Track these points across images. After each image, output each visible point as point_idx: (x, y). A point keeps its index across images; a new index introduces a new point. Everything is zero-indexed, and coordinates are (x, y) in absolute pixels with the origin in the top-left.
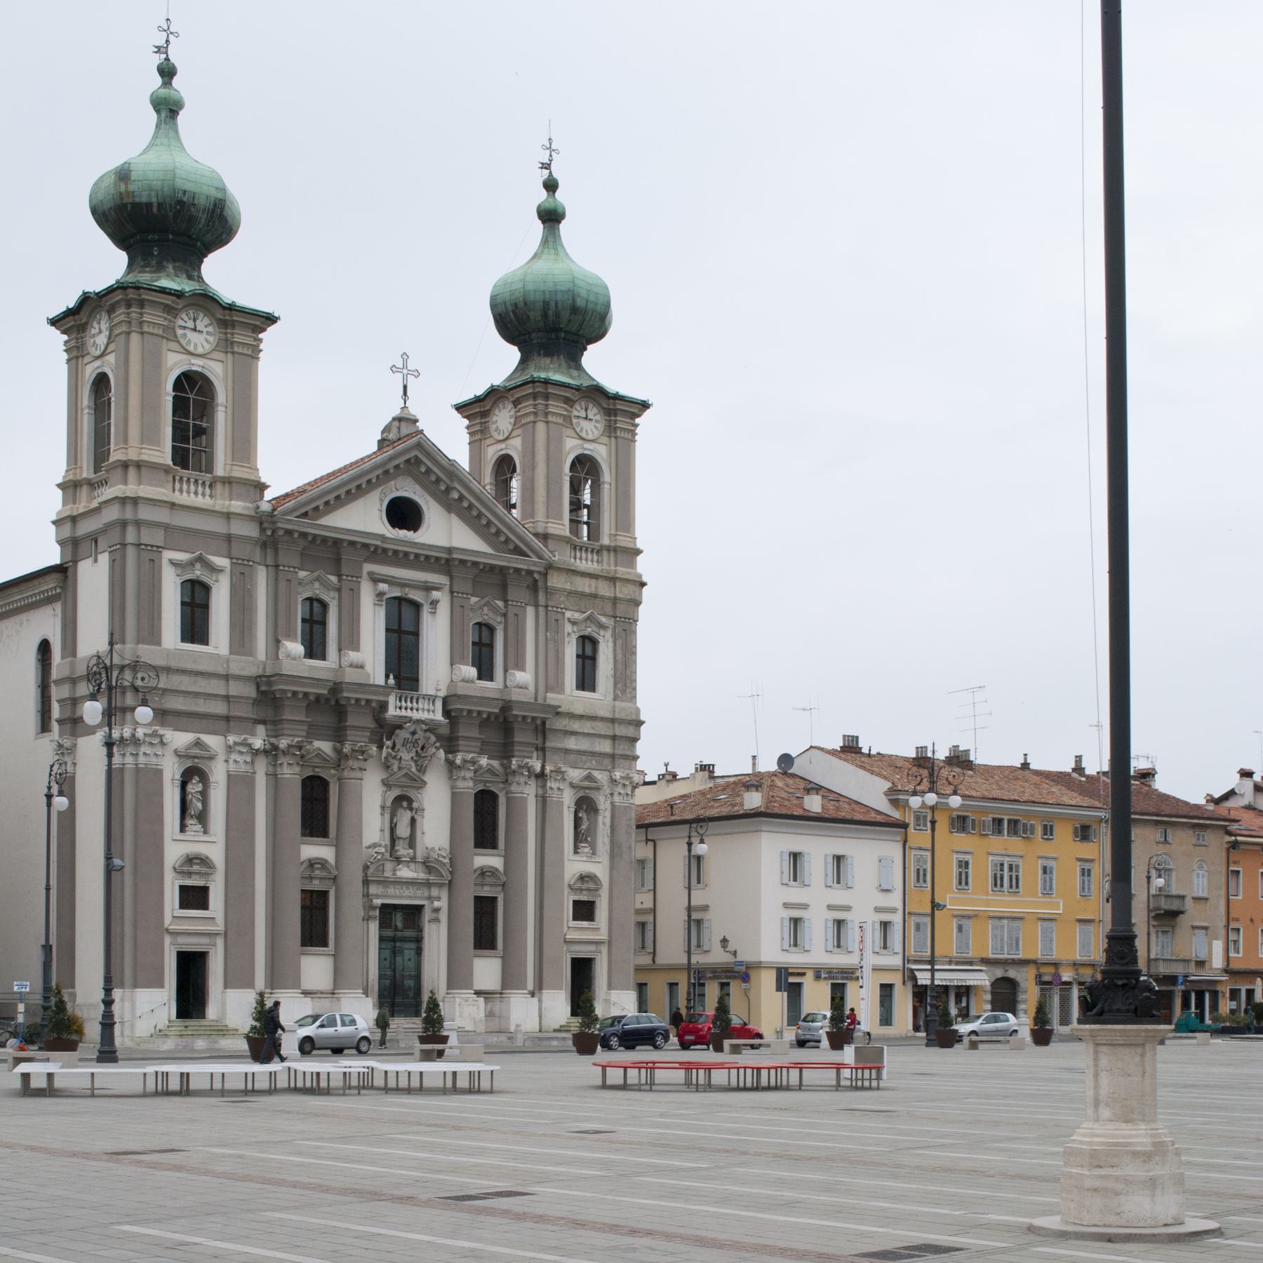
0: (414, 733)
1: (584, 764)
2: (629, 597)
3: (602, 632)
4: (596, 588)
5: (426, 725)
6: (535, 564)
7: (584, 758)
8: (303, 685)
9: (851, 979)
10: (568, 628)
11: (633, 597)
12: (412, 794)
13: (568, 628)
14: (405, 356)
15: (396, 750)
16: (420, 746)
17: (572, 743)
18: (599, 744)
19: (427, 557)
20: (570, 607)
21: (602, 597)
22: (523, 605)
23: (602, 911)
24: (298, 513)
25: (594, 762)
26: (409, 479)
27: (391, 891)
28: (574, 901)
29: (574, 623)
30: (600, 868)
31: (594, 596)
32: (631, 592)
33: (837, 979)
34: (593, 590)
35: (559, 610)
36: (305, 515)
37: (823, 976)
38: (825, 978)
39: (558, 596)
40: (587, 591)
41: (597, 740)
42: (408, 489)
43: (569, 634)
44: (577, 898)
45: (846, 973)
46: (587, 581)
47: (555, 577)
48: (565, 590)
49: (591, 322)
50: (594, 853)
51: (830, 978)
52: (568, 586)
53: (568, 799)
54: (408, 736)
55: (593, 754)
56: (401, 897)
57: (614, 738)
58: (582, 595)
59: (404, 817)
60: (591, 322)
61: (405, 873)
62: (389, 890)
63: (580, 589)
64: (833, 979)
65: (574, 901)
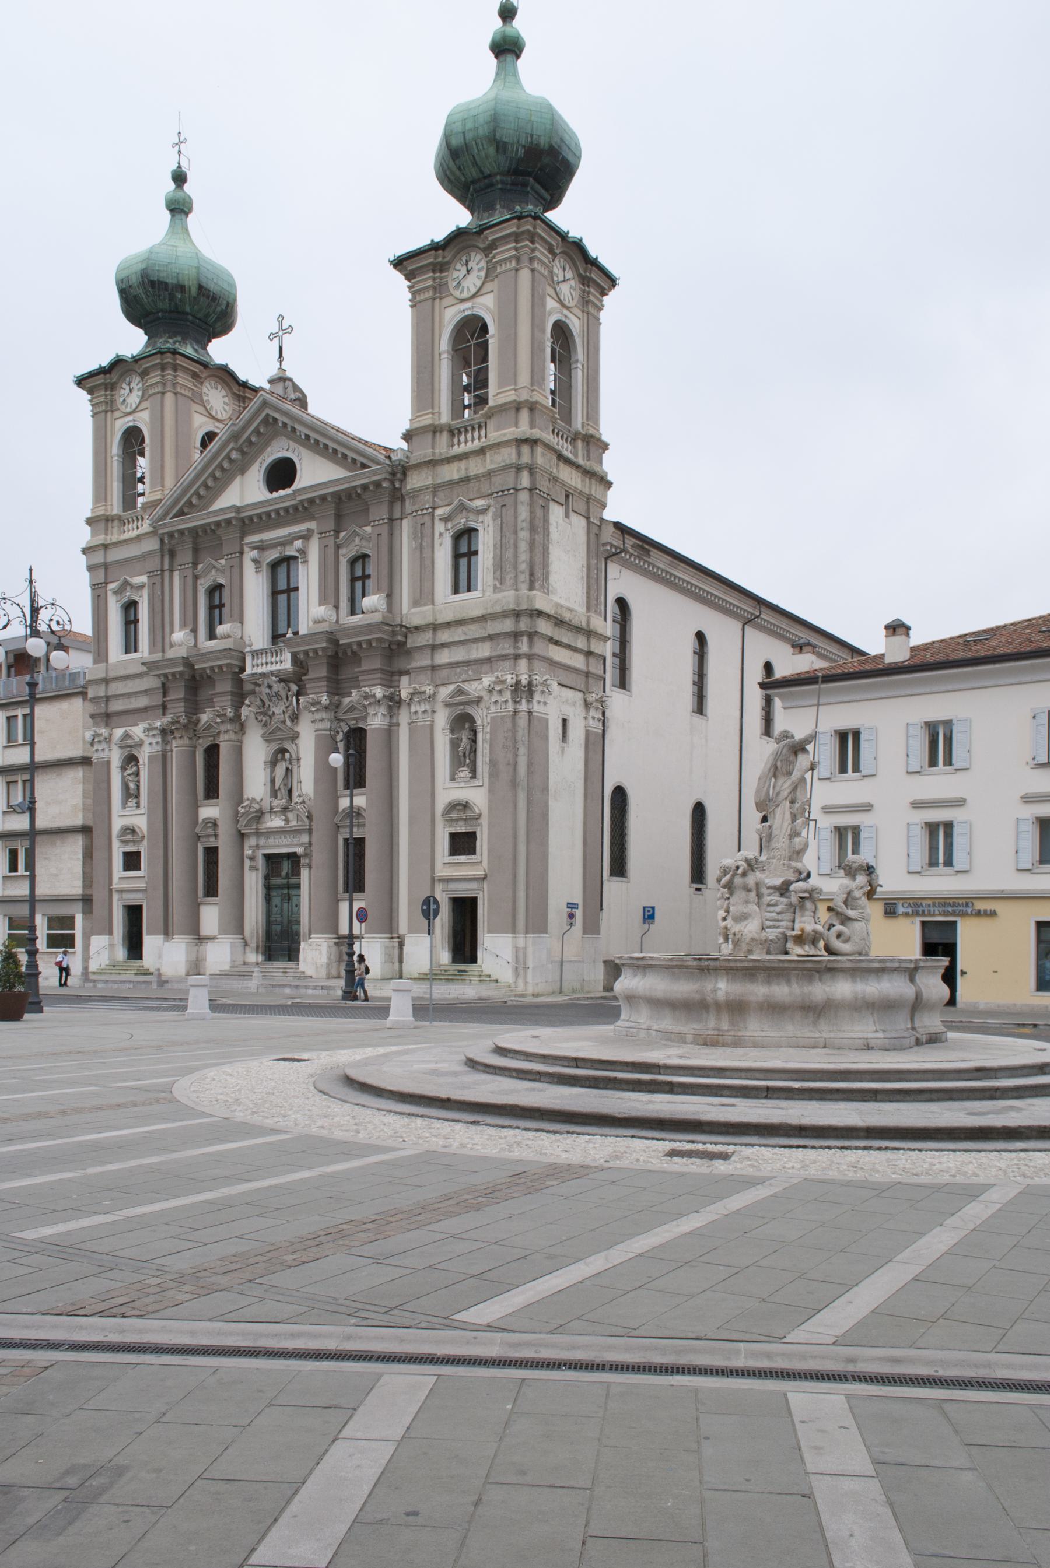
0: (270, 687)
1: (459, 677)
2: (503, 464)
3: (481, 518)
4: (467, 469)
5: (276, 677)
6: (375, 473)
7: (458, 670)
8: (217, 659)
9: (964, 915)
10: (440, 527)
11: (508, 462)
12: (288, 745)
13: (440, 527)
14: (281, 318)
15: (267, 706)
16: (284, 697)
17: (444, 657)
18: (477, 649)
19: (286, 510)
20: (440, 503)
21: (477, 477)
22: (430, 510)
23: (482, 844)
24: (171, 515)
25: (470, 673)
26: (284, 438)
27: (271, 841)
28: (450, 834)
29: (446, 519)
30: (477, 796)
31: (467, 480)
32: (506, 456)
33: (934, 915)
34: (463, 474)
35: (425, 512)
36: (181, 513)
37: (901, 910)
38: (906, 915)
39: (422, 497)
40: (456, 477)
41: (475, 646)
42: (278, 450)
43: (441, 535)
44: (453, 830)
45: (953, 905)
46: (455, 466)
47: (415, 477)
48: (427, 487)
49: (483, 154)
50: (474, 777)
51: (916, 914)
52: (430, 481)
53: (442, 719)
54: (268, 690)
55: (468, 663)
56: (278, 846)
57: (490, 638)
58: (452, 484)
59: (280, 770)
60: (483, 154)
61: (275, 822)
62: (269, 840)
63: (447, 479)
64: (923, 914)
65: (450, 834)
